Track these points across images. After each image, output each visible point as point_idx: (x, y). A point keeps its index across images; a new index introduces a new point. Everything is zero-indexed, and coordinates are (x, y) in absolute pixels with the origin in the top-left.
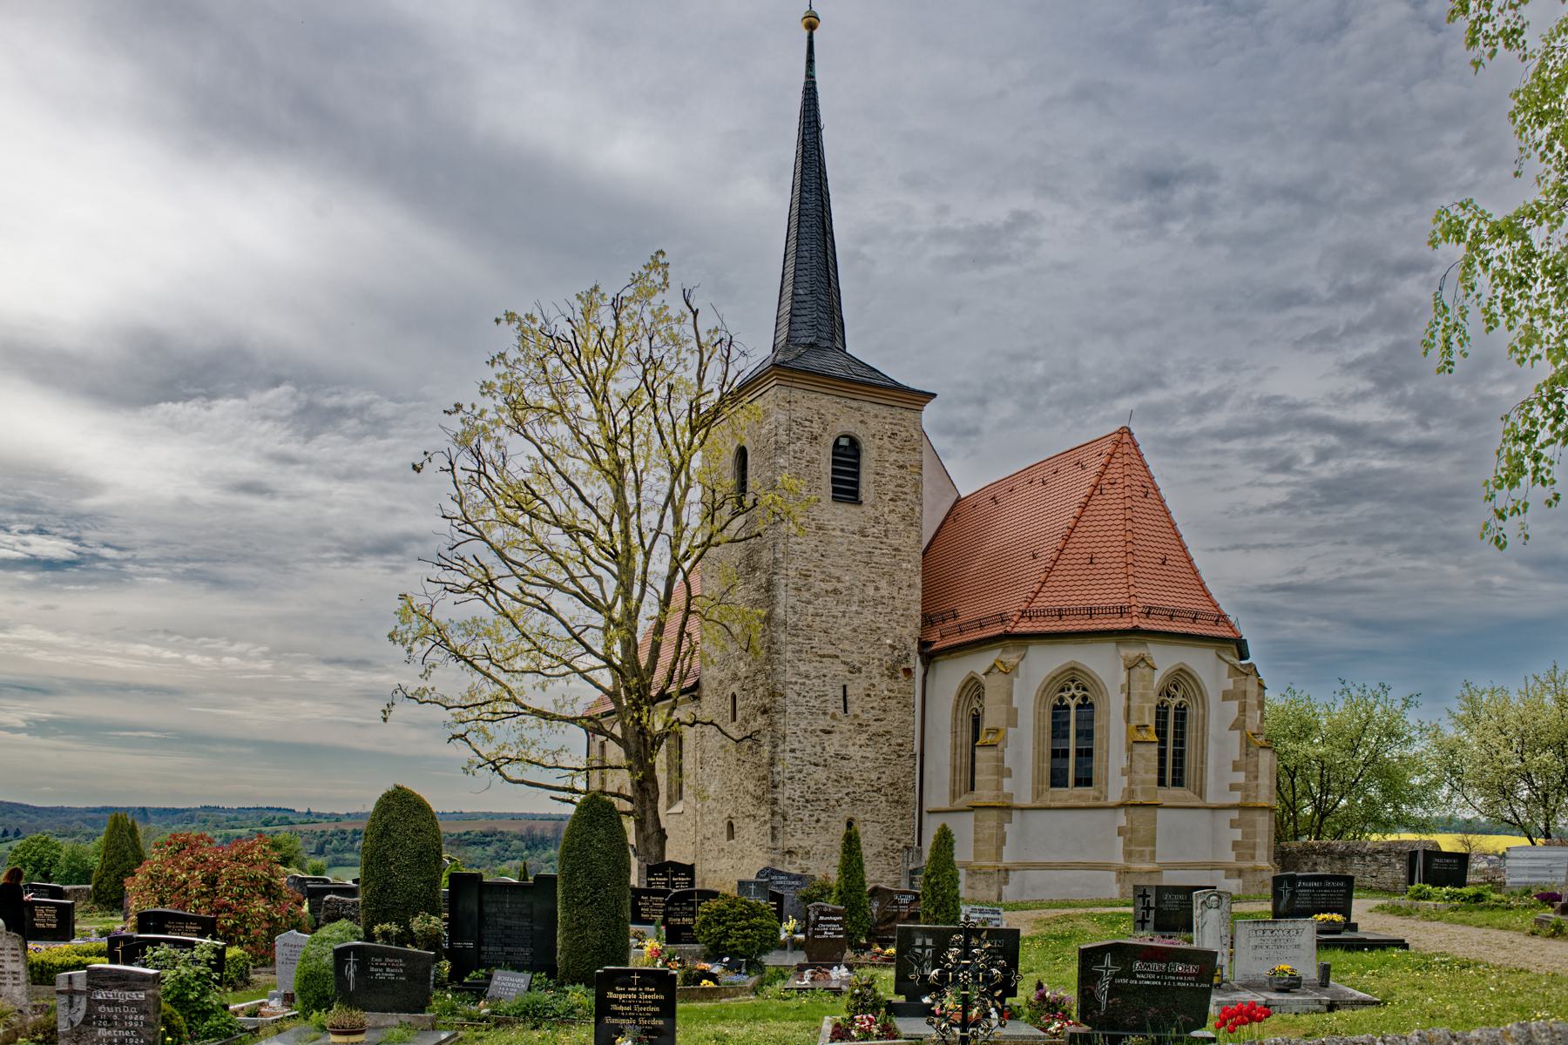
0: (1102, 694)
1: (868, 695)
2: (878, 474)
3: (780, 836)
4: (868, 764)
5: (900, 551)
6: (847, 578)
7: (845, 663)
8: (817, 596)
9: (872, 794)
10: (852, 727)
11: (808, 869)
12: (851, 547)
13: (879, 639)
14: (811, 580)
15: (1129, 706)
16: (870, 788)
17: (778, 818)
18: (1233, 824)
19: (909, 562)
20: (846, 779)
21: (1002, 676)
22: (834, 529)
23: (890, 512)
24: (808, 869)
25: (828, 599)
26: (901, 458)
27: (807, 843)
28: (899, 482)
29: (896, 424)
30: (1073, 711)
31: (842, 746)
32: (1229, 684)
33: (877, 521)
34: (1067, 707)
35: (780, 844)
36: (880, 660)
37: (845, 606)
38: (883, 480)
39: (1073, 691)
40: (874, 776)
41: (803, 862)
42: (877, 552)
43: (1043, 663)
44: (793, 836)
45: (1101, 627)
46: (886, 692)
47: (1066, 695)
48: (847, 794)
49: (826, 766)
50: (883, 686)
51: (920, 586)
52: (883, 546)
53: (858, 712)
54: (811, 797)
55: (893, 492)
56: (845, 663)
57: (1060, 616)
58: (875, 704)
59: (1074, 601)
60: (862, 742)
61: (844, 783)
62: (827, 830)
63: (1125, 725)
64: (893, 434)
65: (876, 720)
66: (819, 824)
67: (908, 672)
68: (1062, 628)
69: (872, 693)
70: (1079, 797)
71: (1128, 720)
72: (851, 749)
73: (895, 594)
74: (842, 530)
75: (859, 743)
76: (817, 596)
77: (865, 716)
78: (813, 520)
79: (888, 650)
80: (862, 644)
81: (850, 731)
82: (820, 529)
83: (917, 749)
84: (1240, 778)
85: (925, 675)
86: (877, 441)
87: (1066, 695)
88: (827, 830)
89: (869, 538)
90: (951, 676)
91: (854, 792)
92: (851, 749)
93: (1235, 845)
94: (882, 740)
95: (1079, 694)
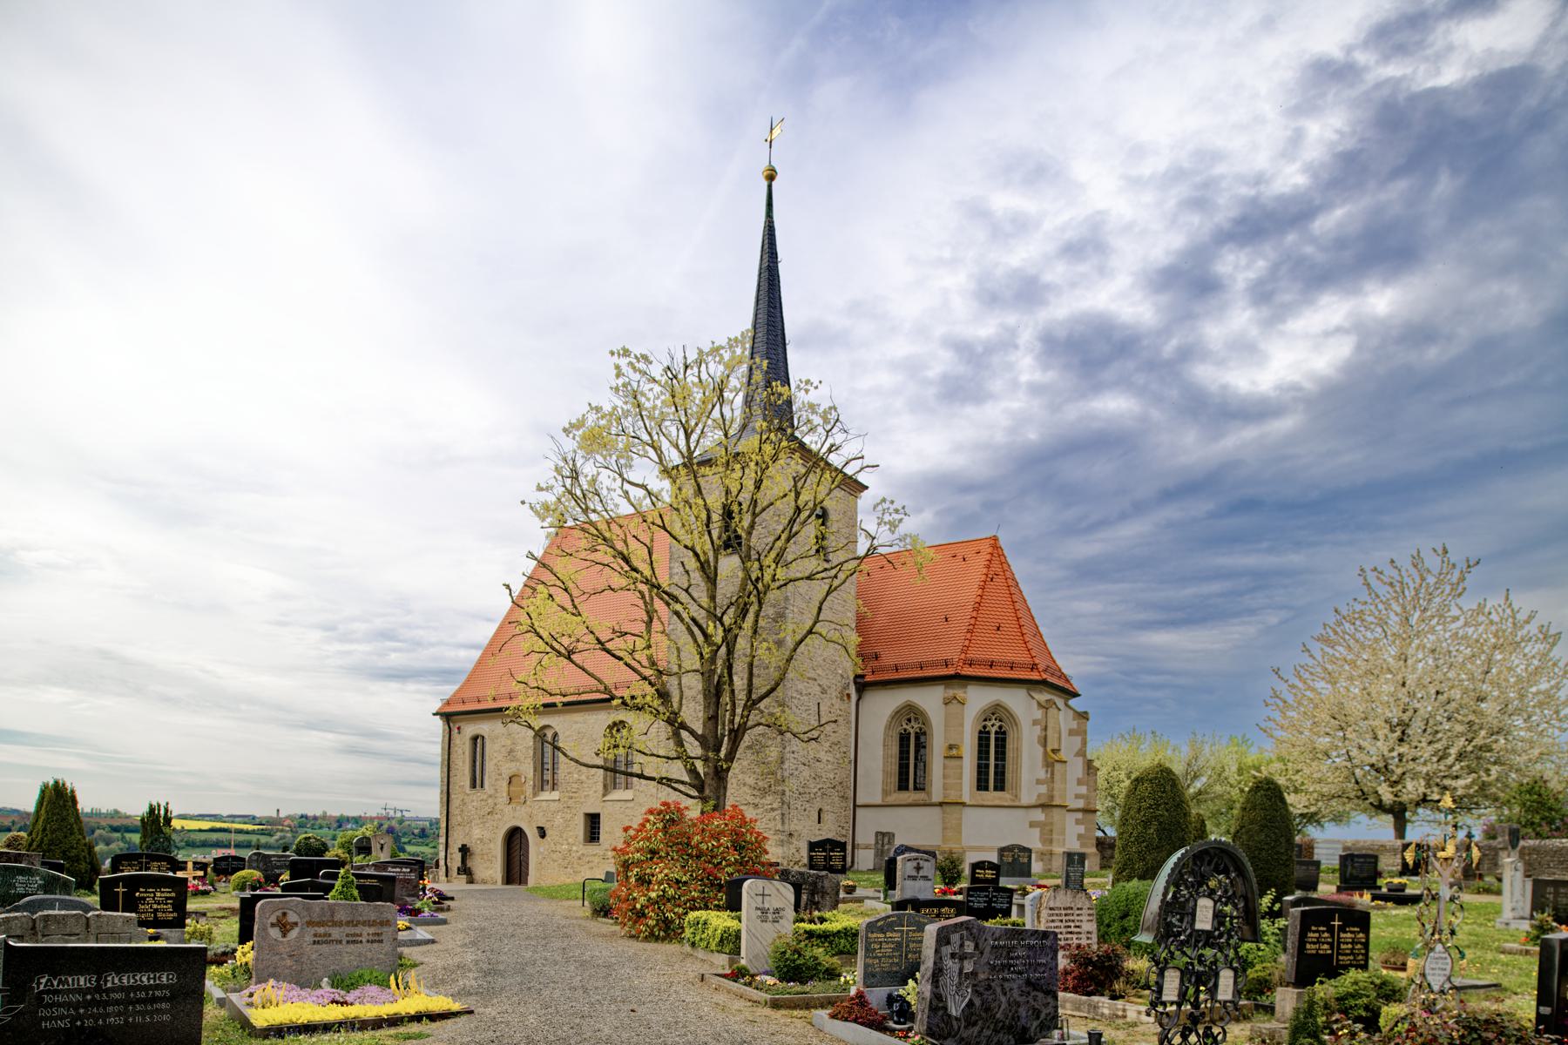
0: (1016, 725)
3: (786, 821)
7: (820, 685)
15: (1046, 736)
17: (785, 806)
18: (1078, 822)
21: (959, 705)
27: (799, 828)
30: (993, 736)
32: (1074, 725)
34: (988, 733)
35: (786, 827)
39: (993, 721)
40: (832, 777)
43: (978, 699)
45: (1021, 677)
47: (989, 724)
54: (801, 790)
56: (820, 685)
57: (1012, 668)
59: (994, 655)
63: (1041, 749)
67: (849, 696)
68: (990, 675)
70: (1000, 798)
71: (1045, 746)
79: (839, 678)
83: (852, 757)
84: (1083, 790)
85: (858, 700)
87: (989, 724)
90: (883, 706)
93: (1080, 837)
94: (836, 748)
95: (998, 724)
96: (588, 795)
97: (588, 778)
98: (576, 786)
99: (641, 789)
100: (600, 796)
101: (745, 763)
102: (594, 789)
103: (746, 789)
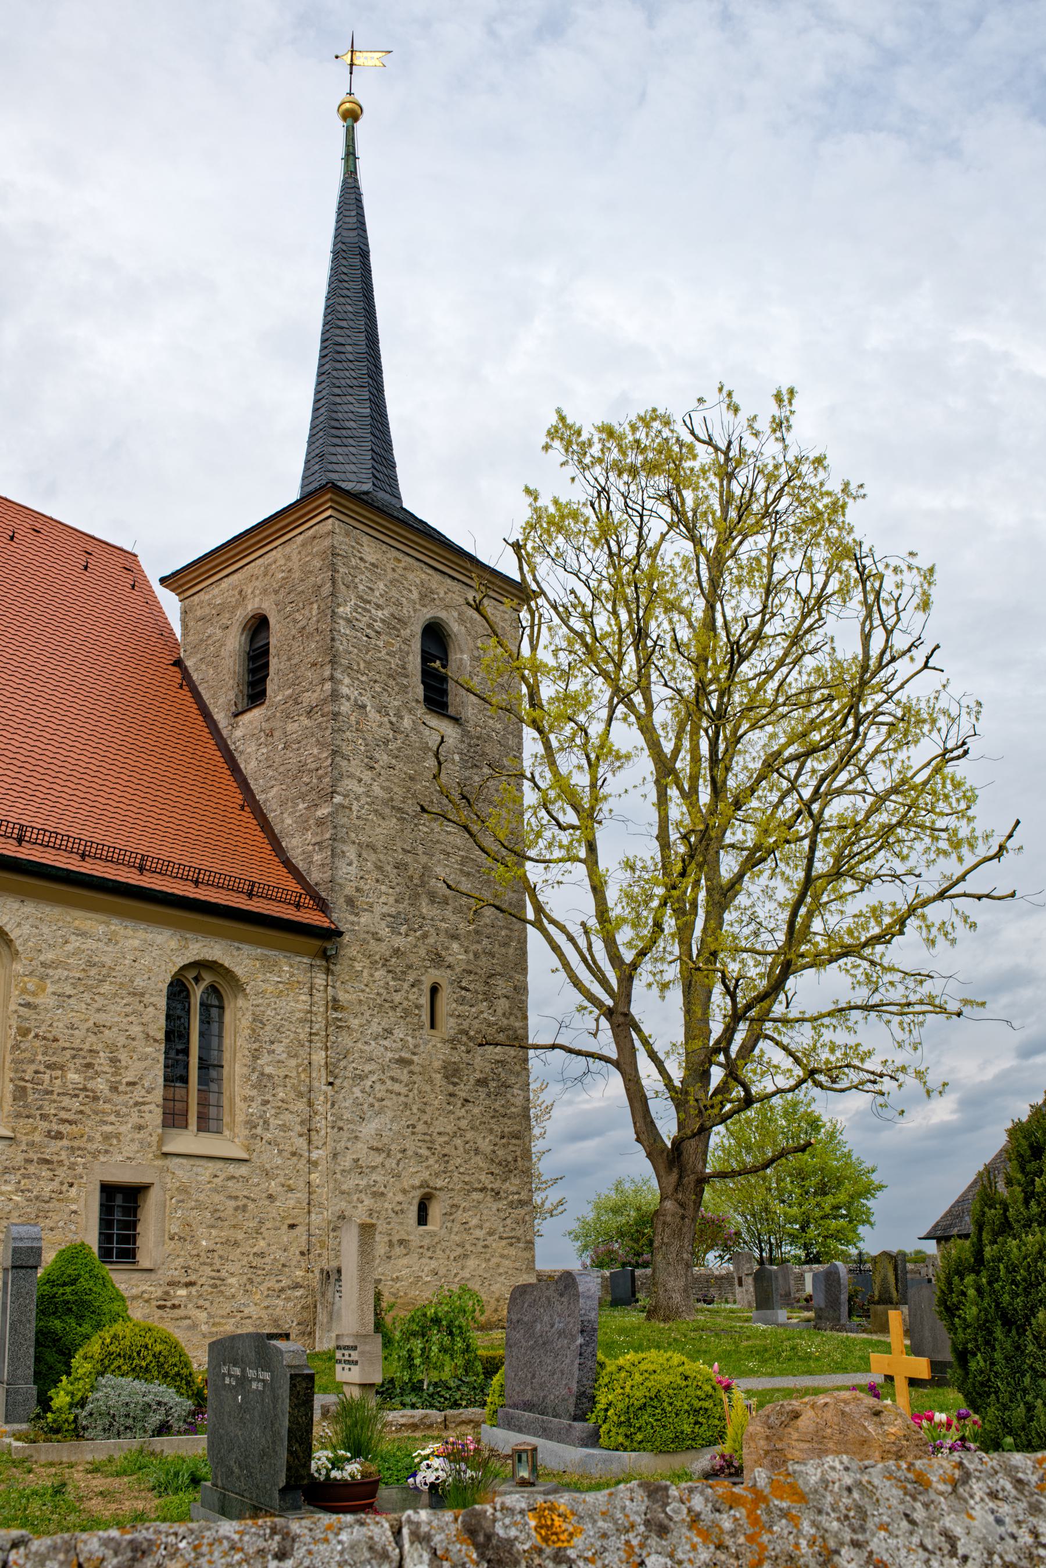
96: (118, 1135)
97: (114, 1089)
98: (75, 1104)
99: (268, 1136)
100: (155, 1138)
101: (476, 1111)
102: (134, 1119)
103: (478, 1160)
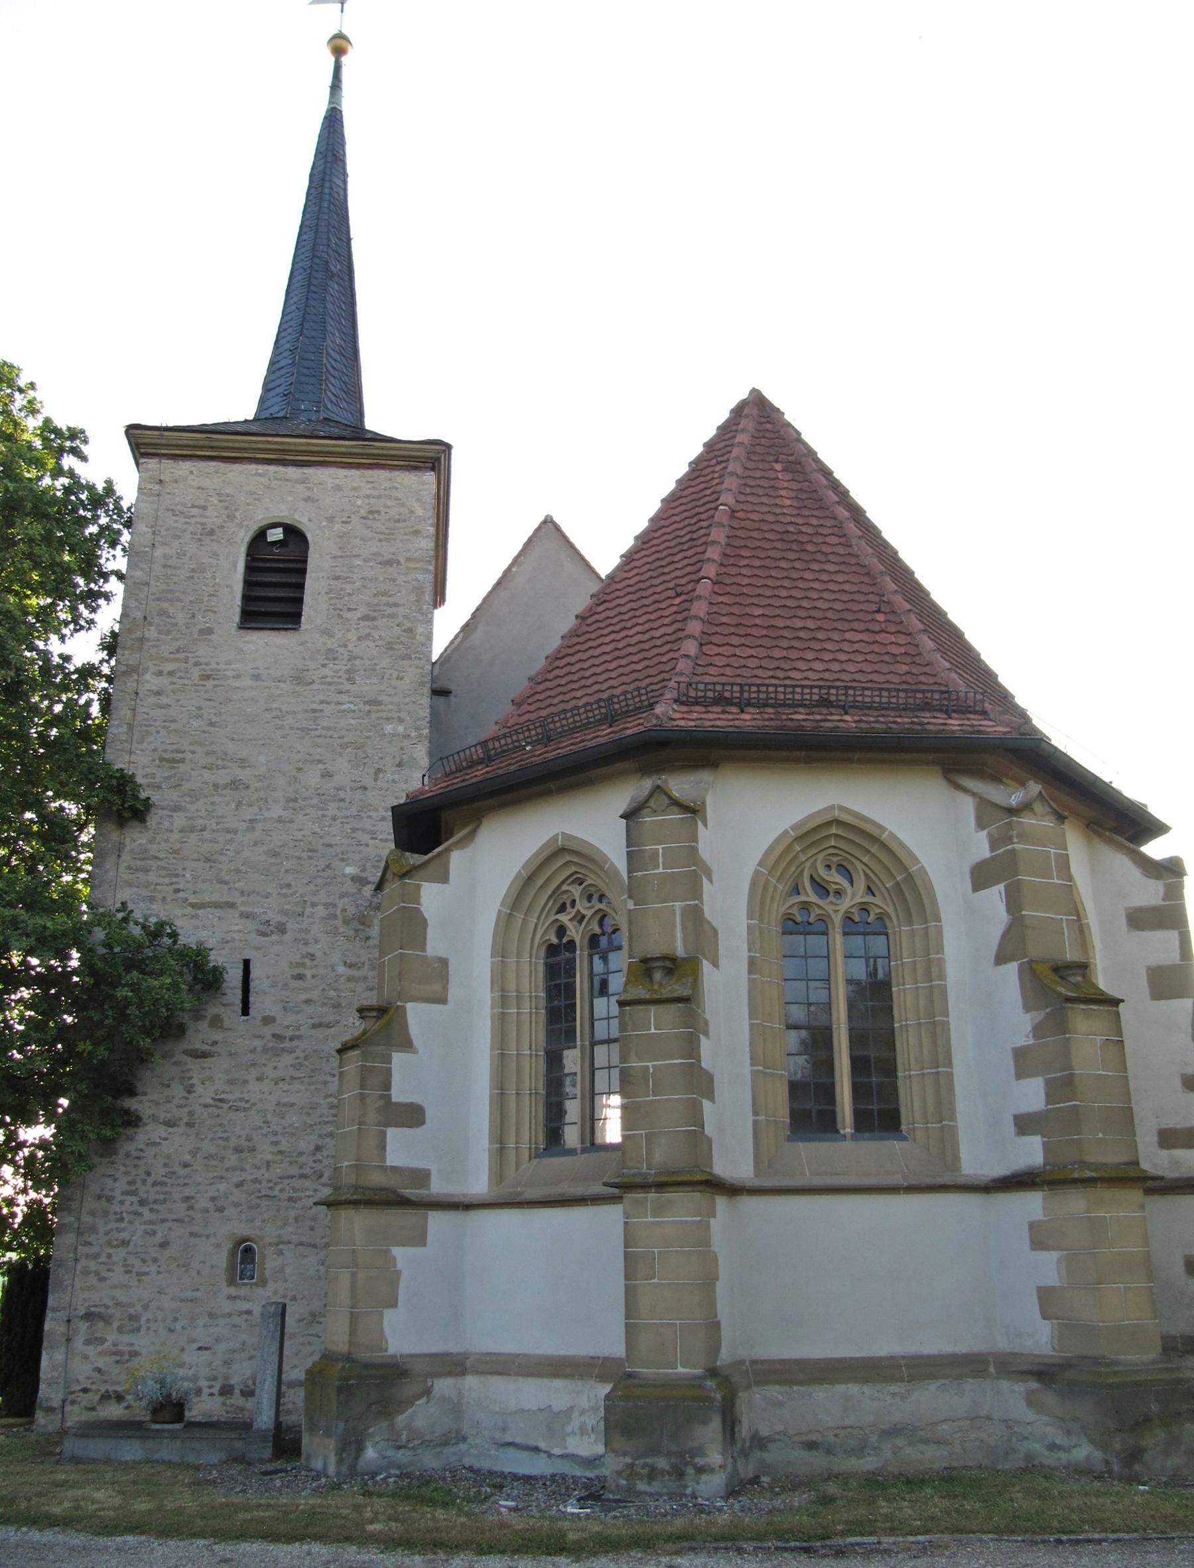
1: (300, 977)
2: (337, 578)
4: (294, 1119)
5: (379, 703)
6: (262, 759)
8: (194, 795)
9: (297, 1183)
10: (258, 1043)
11: (134, 1354)
12: (274, 705)
13: (328, 866)
14: (182, 768)
16: (294, 1171)
19: (401, 720)
20: (238, 1150)
22: (238, 676)
23: (360, 639)
24: (134, 1354)
25: (217, 799)
26: (387, 550)
28: (383, 587)
29: (379, 497)
31: (231, 1082)
33: (331, 656)
36: (326, 905)
37: (255, 809)
38: (349, 588)
40: (305, 1144)
41: (126, 1338)
42: (328, 709)
44: (102, 1279)
46: (341, 969)
48: (239, 1185)
49: (190, 1125)
50: (336, 957)
51: (425, 762)
52: (343, 698)
53: (273, 1010)
55: (368, 604)
56: (246, 916)
58: (315, 995)
60: (279, 1073)
61: (233, 1160)
62: (186, 1266)
64: (371, 512)
65: (314, 1026)
66: (168, 1253)
69: (308, 973)
72: (255, 1087)
73: (368, 781)
74: (257, 677)
75: (271, 1074)
76: (194, 795)
77: (290, 1019)
78: (196, 664)
79: (350, 887)
80: (289, 878)
81: (253, 1050)
82: (208, 677)
86: (337, 527)
88: (186, 1266)
89: (315, 686)
91: (256, 1181)
92: (255, 1087)
